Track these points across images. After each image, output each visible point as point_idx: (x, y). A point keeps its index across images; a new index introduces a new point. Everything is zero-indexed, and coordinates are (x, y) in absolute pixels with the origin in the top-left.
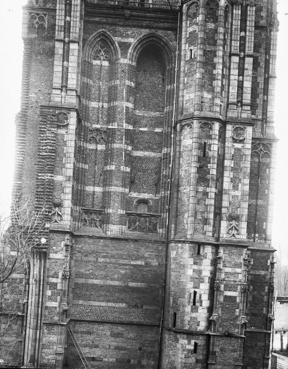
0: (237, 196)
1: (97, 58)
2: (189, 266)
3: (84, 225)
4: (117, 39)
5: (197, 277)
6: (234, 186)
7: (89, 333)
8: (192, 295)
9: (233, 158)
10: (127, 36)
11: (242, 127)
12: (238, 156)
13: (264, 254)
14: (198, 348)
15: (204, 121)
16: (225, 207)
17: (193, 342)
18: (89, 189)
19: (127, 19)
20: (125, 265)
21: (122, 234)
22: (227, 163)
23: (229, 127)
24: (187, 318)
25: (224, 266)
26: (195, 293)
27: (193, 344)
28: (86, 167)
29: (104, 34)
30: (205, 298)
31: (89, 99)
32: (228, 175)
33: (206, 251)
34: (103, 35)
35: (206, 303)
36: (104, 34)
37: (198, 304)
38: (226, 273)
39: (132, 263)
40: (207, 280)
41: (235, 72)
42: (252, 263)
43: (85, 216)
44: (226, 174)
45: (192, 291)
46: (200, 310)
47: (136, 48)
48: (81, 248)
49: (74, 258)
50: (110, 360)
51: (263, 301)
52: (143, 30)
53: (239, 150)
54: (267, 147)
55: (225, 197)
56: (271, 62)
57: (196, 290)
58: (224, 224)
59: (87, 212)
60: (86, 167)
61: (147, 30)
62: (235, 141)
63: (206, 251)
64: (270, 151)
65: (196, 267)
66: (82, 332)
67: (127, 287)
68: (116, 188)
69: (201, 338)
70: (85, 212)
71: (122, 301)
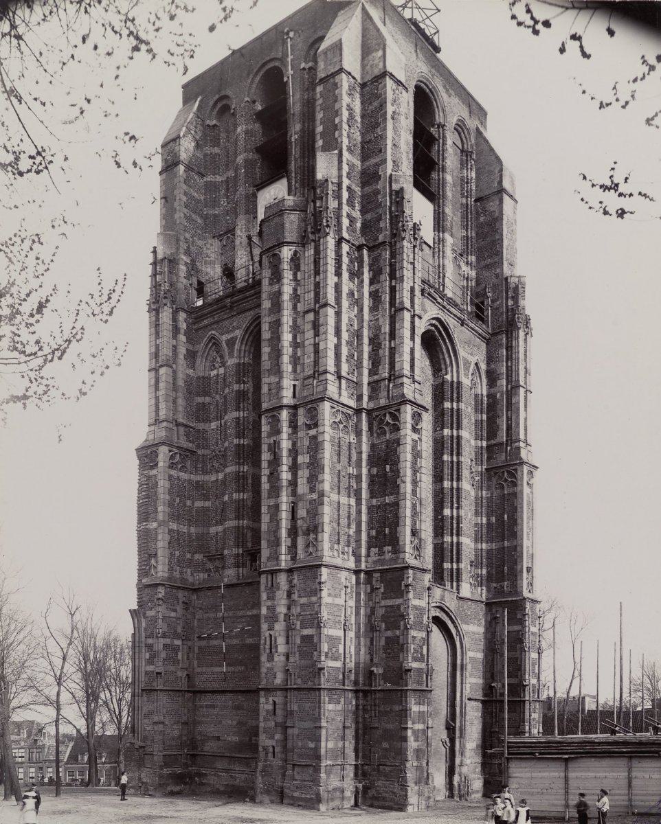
0: (315, 500)
1: (213, 367)
2: (263, 603)
3: (209, 576)
4: (224, 338)
5: (271, 615)
6: (311, 488)
7: (213, 706)
8: (268, 639)
9: (310, 450)
10: (234, 328)
11: (314, 405)
12: (315, 446)
13: (397, 574)
14: (277, 706)
15: (269, 415)
16: (302, 518)
17: (271, 699)
18: (213, 530)
19: (231, 308)
20: (241, 617)
21: (238, 579)
22: (300, 459)
23: (301, 411)
24: (264, 670)
25: (300, 596)
26: (271, 635)
27: (271, 702)
28: (207, 504)
29: (213, 338)
30: (281, 640)
31: (207, 420)
32: (303, 474)
33: (279, 581)
34: (213, 338)
35: (282, 648)
36: (213, 338)
37: (273, 650)
38: (302, 605)
39: (249, 613)
40: (282, 617)
41: (310, 334)
42: (382, 590)
43: (209, 565)
44: (300, 473)
45: (267, 635)
46: (276, 659)
47: (243, 339)
48: (202, 604)
49: (197, 617)
50: (234, 739)
51: (398, 643)
52: (248, 314)
53: (314, 438)
54: (395, 415)
55: (300, 505)
56: (397, 289)
57: (272, 632)
58: (300, 541)
59: (211, 558)
60: (207, 504)
61: (252, 313)
62: (309, 427)
63: (279, 581)
64: (398, 421)
65: (269, 603)
66: (207, 706)
67: (246, 645)
68: (230, 522)
69: (279, 693)
70: (210, 560)
71: (241, 663)
